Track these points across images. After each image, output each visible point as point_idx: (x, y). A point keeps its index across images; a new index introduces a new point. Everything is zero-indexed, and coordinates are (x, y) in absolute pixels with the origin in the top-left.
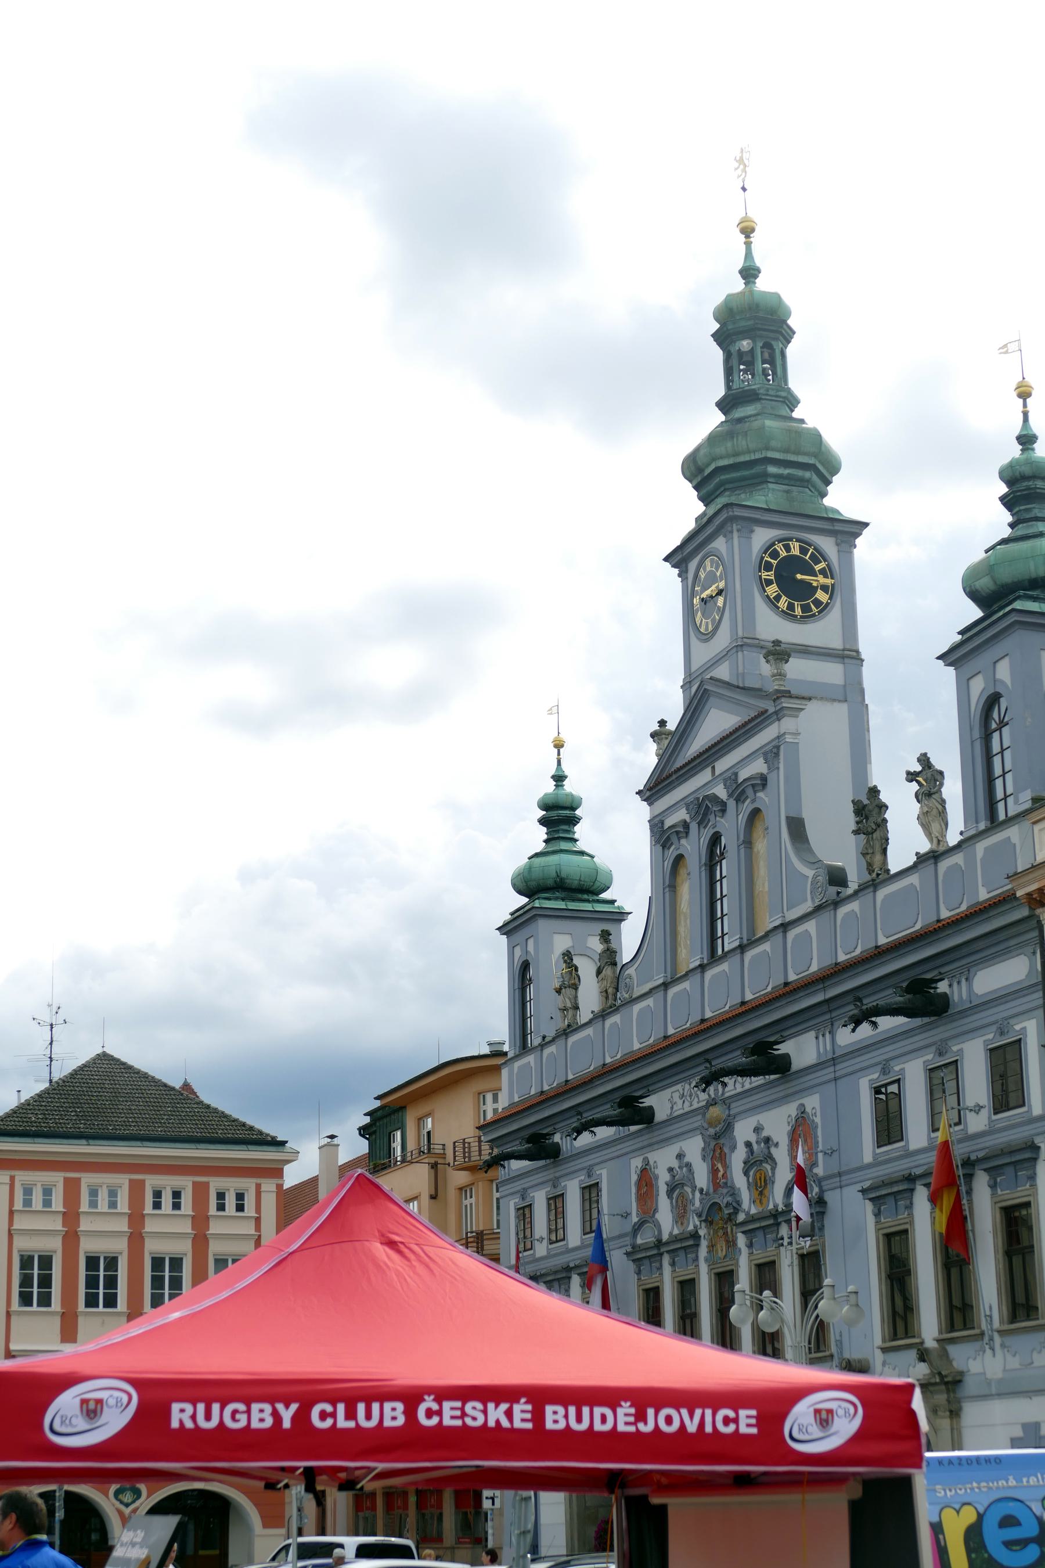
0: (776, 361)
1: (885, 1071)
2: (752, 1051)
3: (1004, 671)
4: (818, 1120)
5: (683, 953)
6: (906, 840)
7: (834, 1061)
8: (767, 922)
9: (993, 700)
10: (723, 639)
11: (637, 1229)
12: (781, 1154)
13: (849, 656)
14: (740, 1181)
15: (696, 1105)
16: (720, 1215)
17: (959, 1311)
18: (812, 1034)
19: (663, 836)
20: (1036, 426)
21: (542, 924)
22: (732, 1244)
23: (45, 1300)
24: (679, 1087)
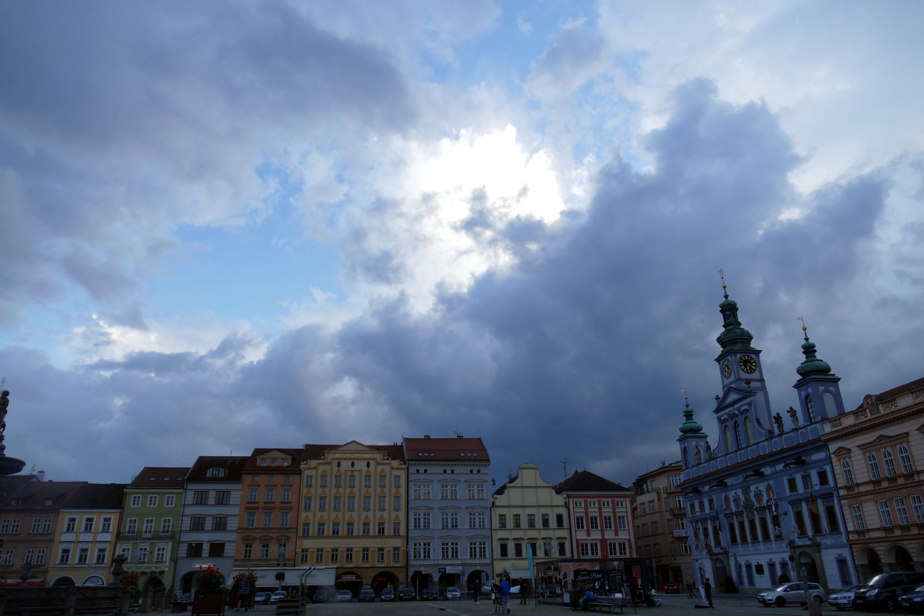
0: (735, 316)
1: (790, 475)
2: (753, 470)
3: (810, 390)
5: (730, 448)
8: (752, 442)
9: (807, 396)
10: (732, 378)
12: (764, 494)
13: (762, 380)
14: (753, 499)
16: (749, 506)
17: (817, 530)
18: (768, 468)
19: (721, 422)
20: (808, 336)
21: (689, 440)
23: (583, 527)
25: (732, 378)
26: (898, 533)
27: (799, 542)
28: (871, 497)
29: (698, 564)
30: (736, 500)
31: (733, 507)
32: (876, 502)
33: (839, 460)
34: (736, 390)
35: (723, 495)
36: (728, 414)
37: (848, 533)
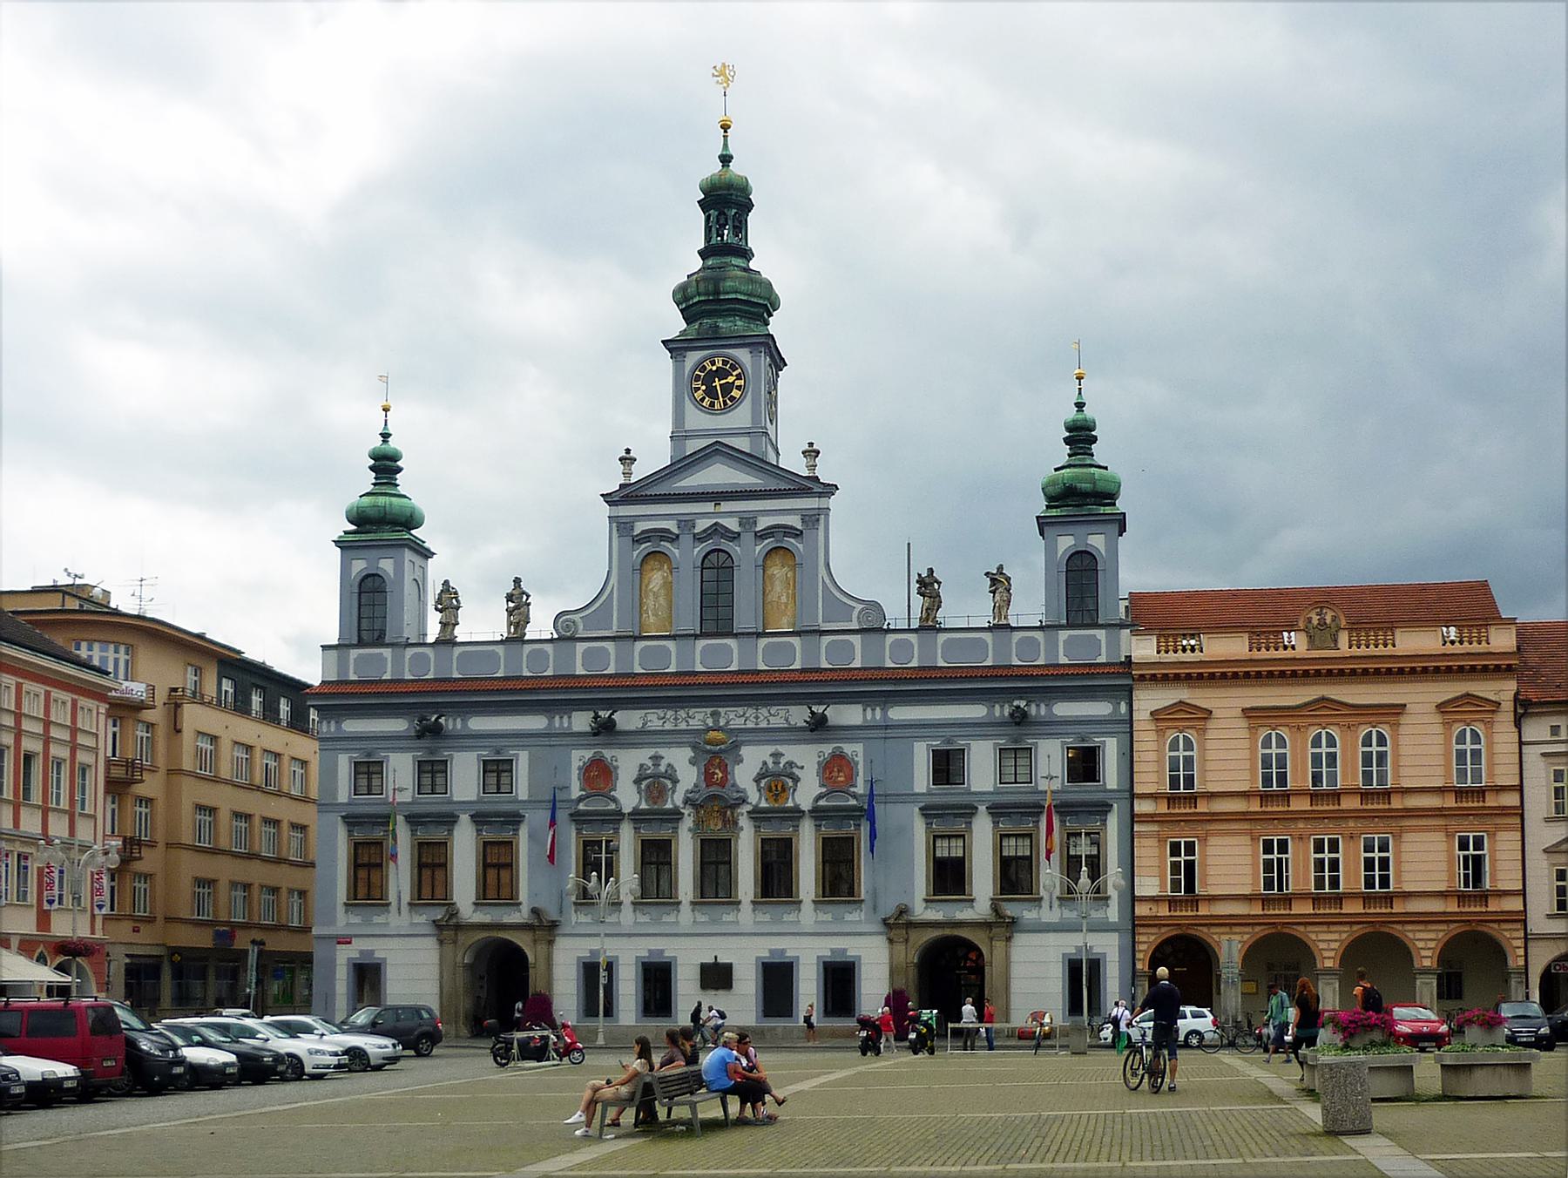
4: (860, 759)
6: (965, 607)
7: (887, 727)
11: (580, 799)
15: (683, 726)
16: (716, 802)
18: (859, 707)
24: (660, 712)
25: (741, 417)
26: (1302, 908)
27: (921, 912)
28: (1246, 826)
29: (344, 956)
30: (655, 782)
31: (628, 796)
32: (1254, 839)
33: (1160, 732)
36: (686, 523)
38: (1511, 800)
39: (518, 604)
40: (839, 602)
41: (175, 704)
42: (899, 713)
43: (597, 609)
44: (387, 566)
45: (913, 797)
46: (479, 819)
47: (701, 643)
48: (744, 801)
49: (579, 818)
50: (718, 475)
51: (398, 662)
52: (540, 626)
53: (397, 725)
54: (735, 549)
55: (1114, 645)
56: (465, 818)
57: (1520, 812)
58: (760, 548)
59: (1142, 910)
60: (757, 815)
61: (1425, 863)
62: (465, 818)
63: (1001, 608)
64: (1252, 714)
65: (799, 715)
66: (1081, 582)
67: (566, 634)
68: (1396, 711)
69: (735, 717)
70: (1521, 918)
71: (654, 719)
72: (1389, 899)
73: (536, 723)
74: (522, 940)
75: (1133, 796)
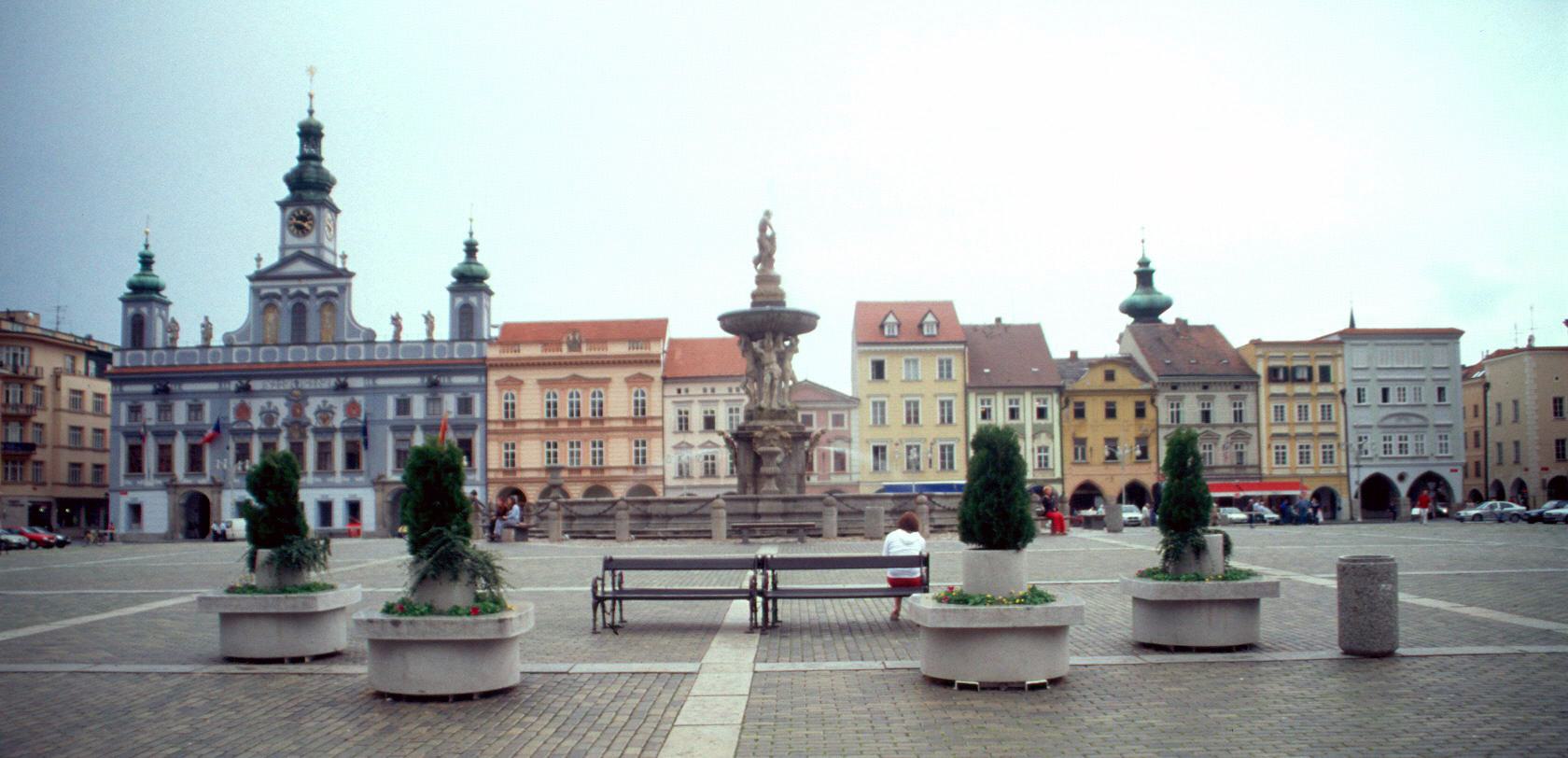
16: (297, 424)
22: (304, 436)
25: (310, 239)
30: (269, 415)
31: (256, 422)
34: (317, 261)
35: (234, 403)
36: (285, 290)
37: (487, 470)
38: (658, 423)
39: (207, 331)
40: (354, 329)
41: (57, 376)
42: (382, 382)
43: (243, 333)
44: (144, 310)
45: (384, 422)
46: (188, 434)
47: (291, 348)
48: (309, 423)
49: (235, 433)
50: (301, 267)
51: (149, 358)
52: (217, 341)
53: (149, 388)
54: (307, 303)
55: (480, 350)
56: (180, 433)
57: (662, 429)
58: (318, 303)
59: (491, 475)
60: (316, 431)
61: (619, 453)
62: (180, 433)
63: (430, 331)
64: (542, 382)
65: (332, 382)
66: (466, 320)
67: (229, 345)
68: (606, 381)
69: (305, 384)
70: (662, 479)
71: (269, 385)
72: (602, 470)
73: (213, 386)
74: (207, 492)
75: (486, 421)
